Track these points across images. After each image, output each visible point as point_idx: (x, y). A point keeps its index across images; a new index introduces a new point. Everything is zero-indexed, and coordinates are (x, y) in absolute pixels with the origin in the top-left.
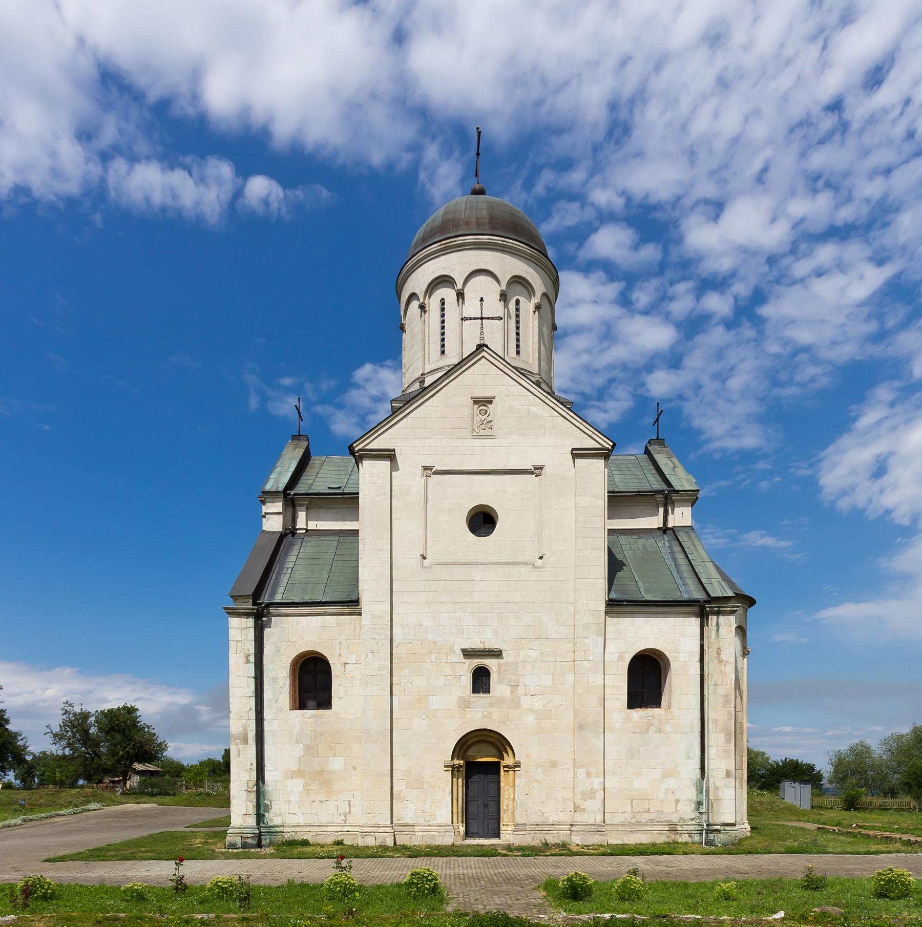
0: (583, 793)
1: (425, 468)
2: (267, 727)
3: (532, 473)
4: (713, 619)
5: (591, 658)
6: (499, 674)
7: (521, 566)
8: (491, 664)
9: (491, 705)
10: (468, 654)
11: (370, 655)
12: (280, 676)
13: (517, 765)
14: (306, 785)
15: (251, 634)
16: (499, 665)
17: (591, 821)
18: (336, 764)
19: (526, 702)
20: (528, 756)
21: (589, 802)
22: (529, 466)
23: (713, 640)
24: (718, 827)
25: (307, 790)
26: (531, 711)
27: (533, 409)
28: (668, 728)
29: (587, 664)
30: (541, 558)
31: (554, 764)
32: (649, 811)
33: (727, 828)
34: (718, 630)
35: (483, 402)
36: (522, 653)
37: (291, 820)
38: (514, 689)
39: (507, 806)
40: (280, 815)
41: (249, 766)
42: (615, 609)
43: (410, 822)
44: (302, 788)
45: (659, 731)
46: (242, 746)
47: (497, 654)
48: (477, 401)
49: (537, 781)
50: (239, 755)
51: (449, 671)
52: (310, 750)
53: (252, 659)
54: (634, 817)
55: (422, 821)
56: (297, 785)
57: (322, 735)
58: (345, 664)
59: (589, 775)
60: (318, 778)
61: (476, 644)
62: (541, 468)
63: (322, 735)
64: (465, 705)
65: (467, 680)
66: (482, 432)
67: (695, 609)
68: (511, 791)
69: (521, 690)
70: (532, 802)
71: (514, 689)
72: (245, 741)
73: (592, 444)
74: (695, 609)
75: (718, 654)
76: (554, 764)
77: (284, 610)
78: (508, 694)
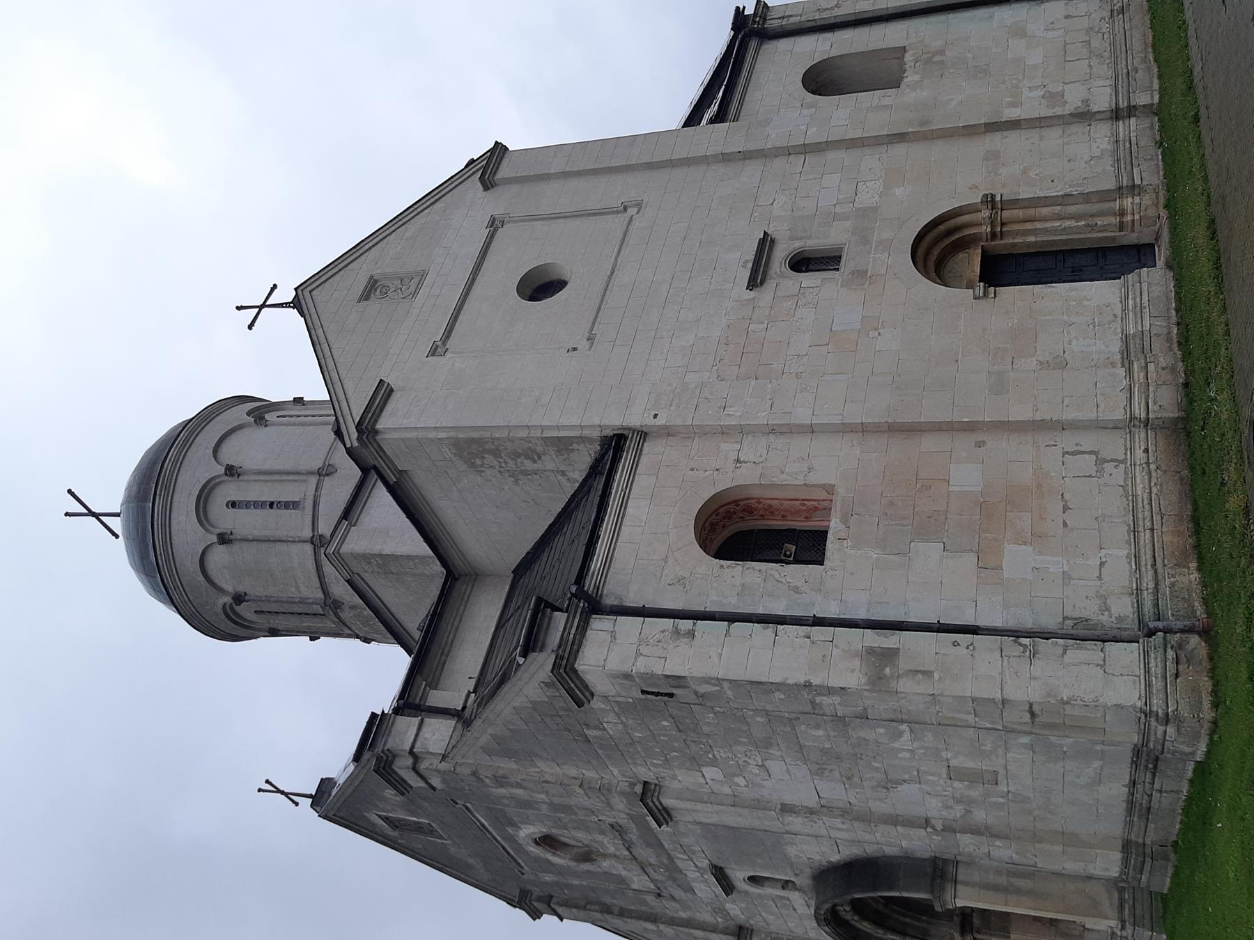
1: (433, 352)
2: (861, 614)
3: (495, 230)
5: (804, 127)
6: (810, 237)
7: (631, 228)
10: (756, 279)
11: (729, 411)
12: (738, 581)
13: (989, 200)
16: (791, 239)
23: (804, 18)
28: (938, 44)
30: (625, 209)
31: (993, 156)
32: (1089, 42)
37: (1119, 572)
39: (1077, 217)
40: (1104, 598)
41: (962, 651)
43: (1116, 346)
44: (1029, 549)
45: (942, 52)
46: (903, 664)
48: (366, 296)
49: (1025, 172)
50: (928, 674)
51: (790, 304)
54: (1100, 56)
55: (1117, 326)
56: (1017, 560)
57: (891, 503)
58: (738, 461)
59: (1013, 105)
63: (891, 503)
65: (809, 279)
66: (412, 289)
68: (1045, 211)
70: (1070, 169)
72: (890, 655)
76: (993, 156)
78: (848, 224)
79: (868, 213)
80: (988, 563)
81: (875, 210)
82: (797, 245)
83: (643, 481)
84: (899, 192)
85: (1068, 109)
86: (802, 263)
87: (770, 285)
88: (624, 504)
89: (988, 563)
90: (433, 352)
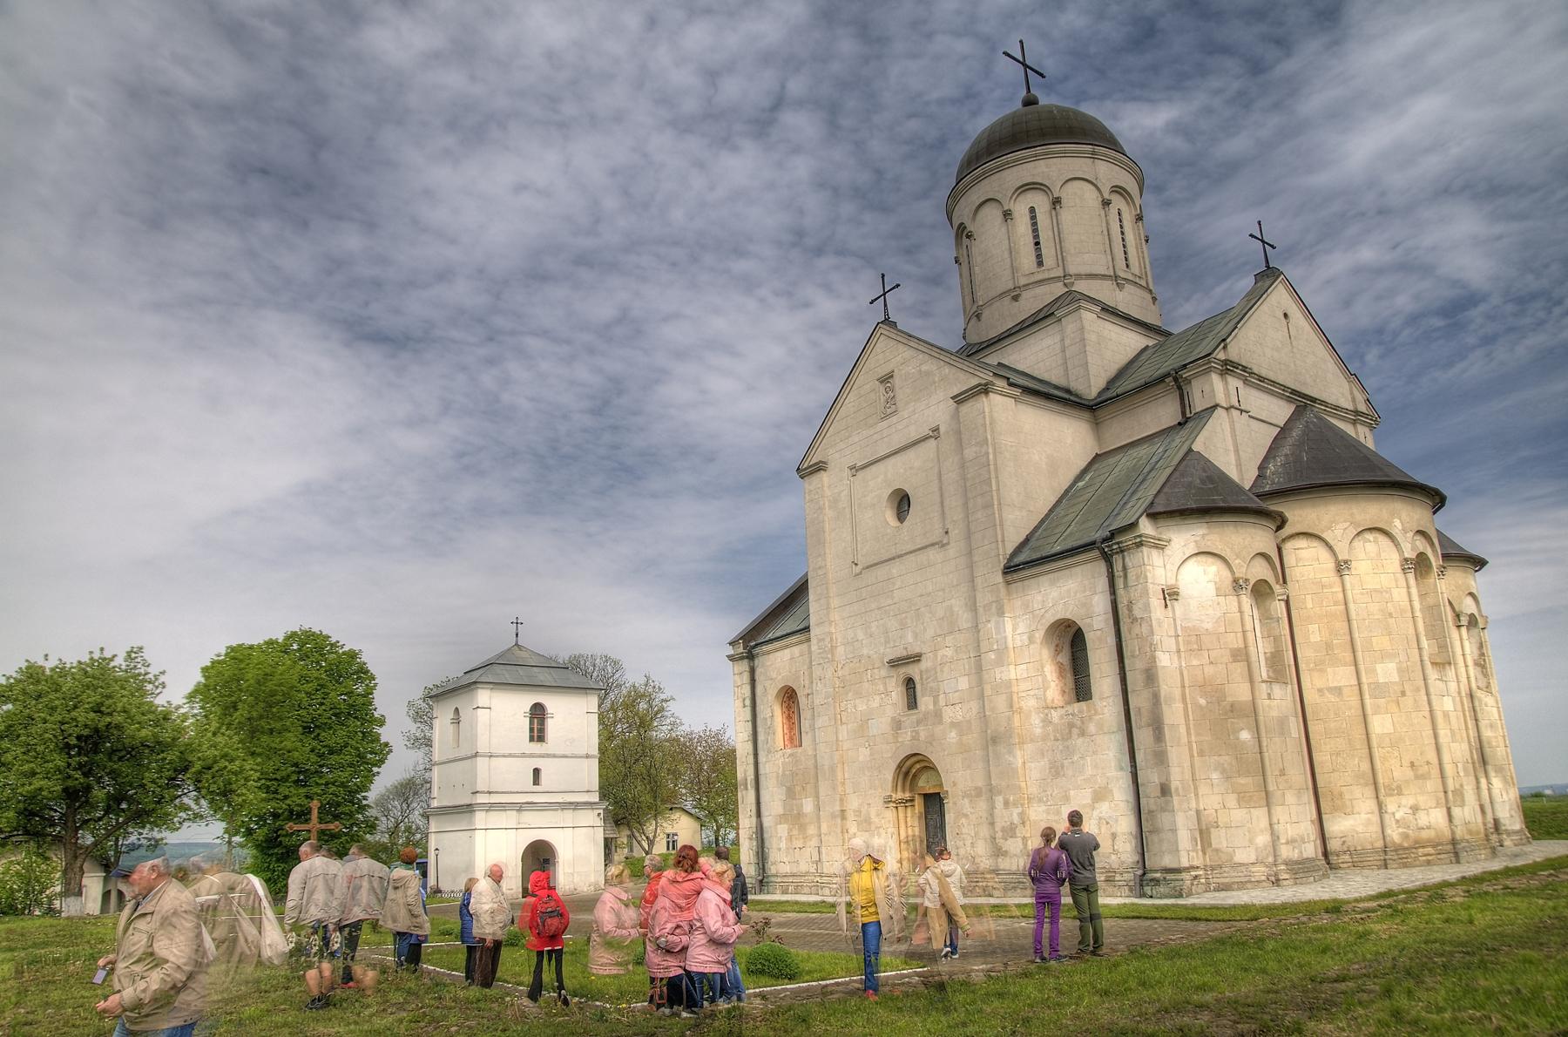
0: (1003, 829)
1: (851, 468)
4: (1118, 562)
8: (913, 671)
9: (918, 723)
10: (895, 663)
14: (790, 830)
15: (746, 677)
17: (1014, 868)
18: (808, 806)
19: (949, 714)
20: (955, 784)
21: (1010, 841)
22: (927, 432)
24: (1158, 875)
25: (790, 838)
26: (953, 725)
27: (924, 368)
28: (1092, 728)
29: (992, 656)
33: (1169, 876)
34: (1126, 576)
35: (886, 379)
36: (940, 653)
38: (936, 703)
42: (1015, 576)
45: (1083, 733)
47: (915, 659)
49: (966, 816)
52: (791, 793)
53: (748, 702)
59: (1006, 804)
60: (794, 818)
61: (900, 652)
62: (936, 429)
64: (897, 725)
65: (897, 694)
67: (1096, 553)
69: (942, 702)
71: (936, 698)
73: (974, 381)
74: (1096, 553)
75: (1130, 610)
77: (765, 648)
79: (938, 715)
80: (782, 818)
81: (940, 722)
82: (917, 679)
83: (796, 650)
84: (953, 734)
85: (1000, 841)
86: (910, 683)
87: (893, 672)
88: (787, 647)
89: (782, 818)
90: (851, 468)
